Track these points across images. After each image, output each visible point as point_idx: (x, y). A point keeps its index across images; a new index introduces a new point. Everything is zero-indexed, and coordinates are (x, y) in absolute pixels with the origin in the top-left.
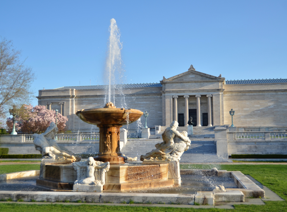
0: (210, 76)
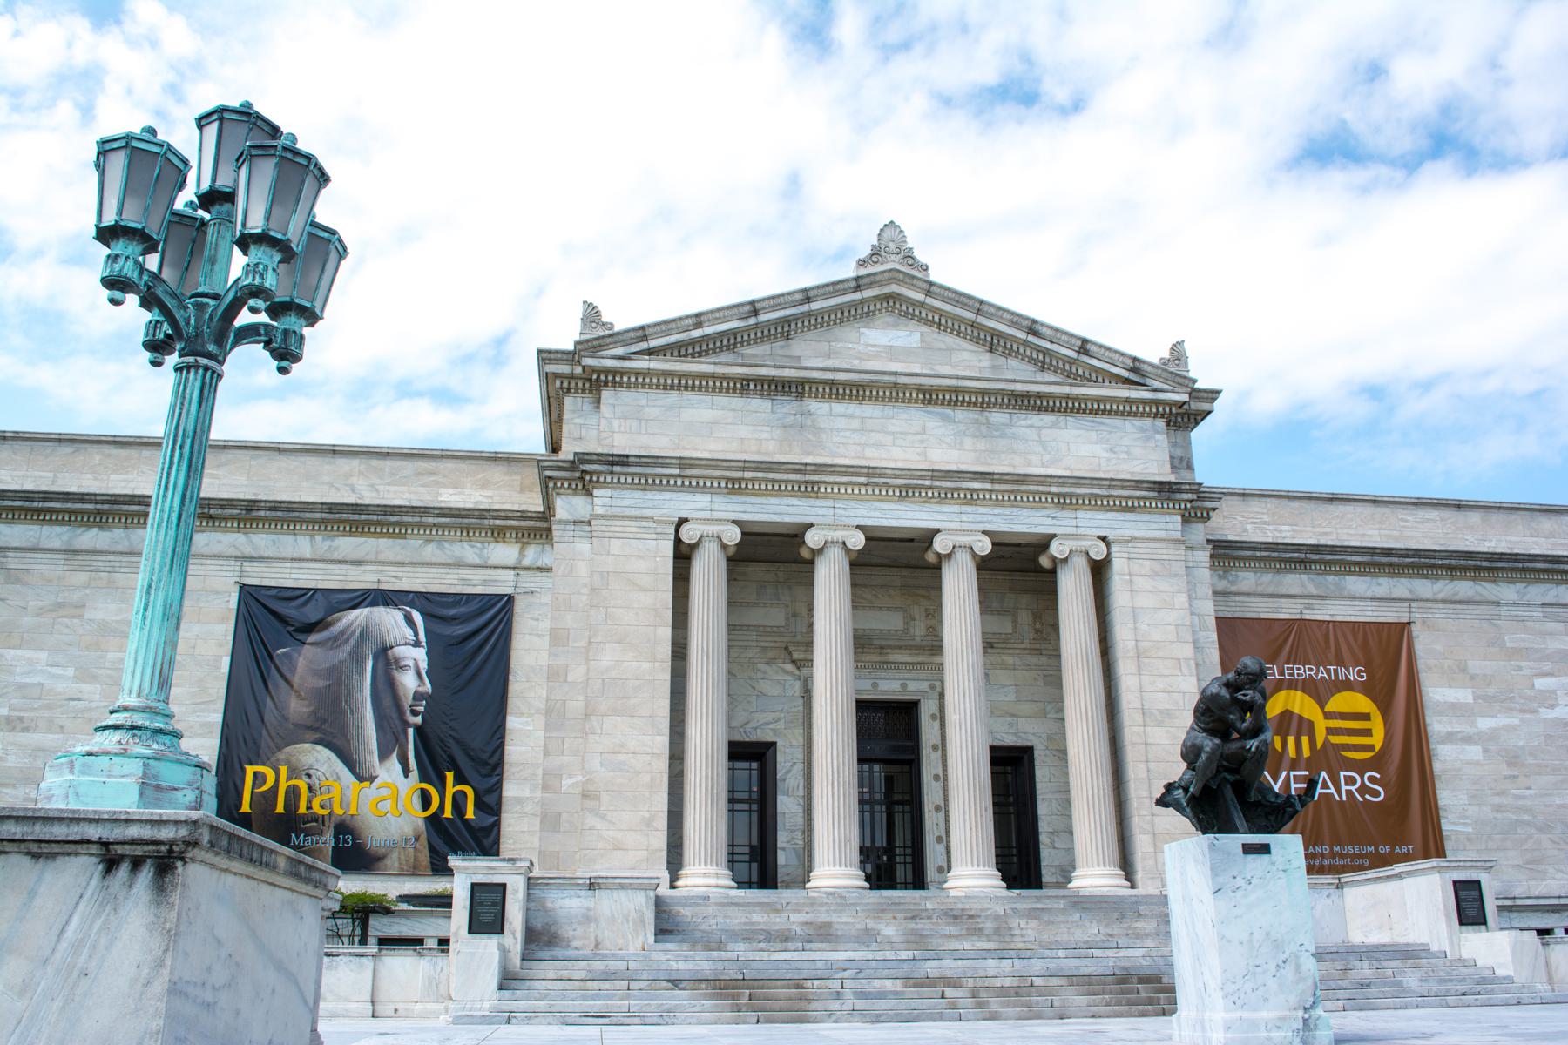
0: (1084, 346)
